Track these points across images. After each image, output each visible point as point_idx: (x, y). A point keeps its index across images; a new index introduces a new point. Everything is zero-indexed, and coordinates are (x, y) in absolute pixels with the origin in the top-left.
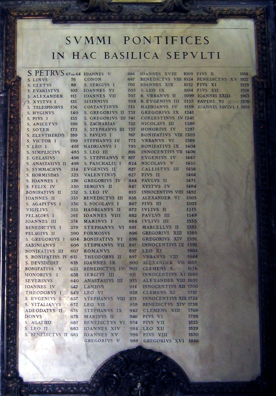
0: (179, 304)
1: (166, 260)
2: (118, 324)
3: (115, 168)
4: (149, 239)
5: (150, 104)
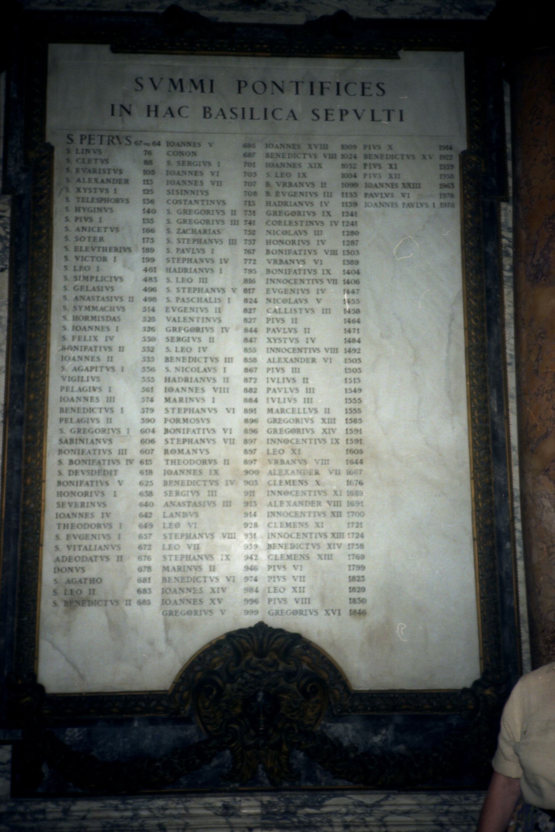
0: (332, 546)
1: (308, 466)
2: (223, 582)
4: (278, 431)
5: (281, 198)
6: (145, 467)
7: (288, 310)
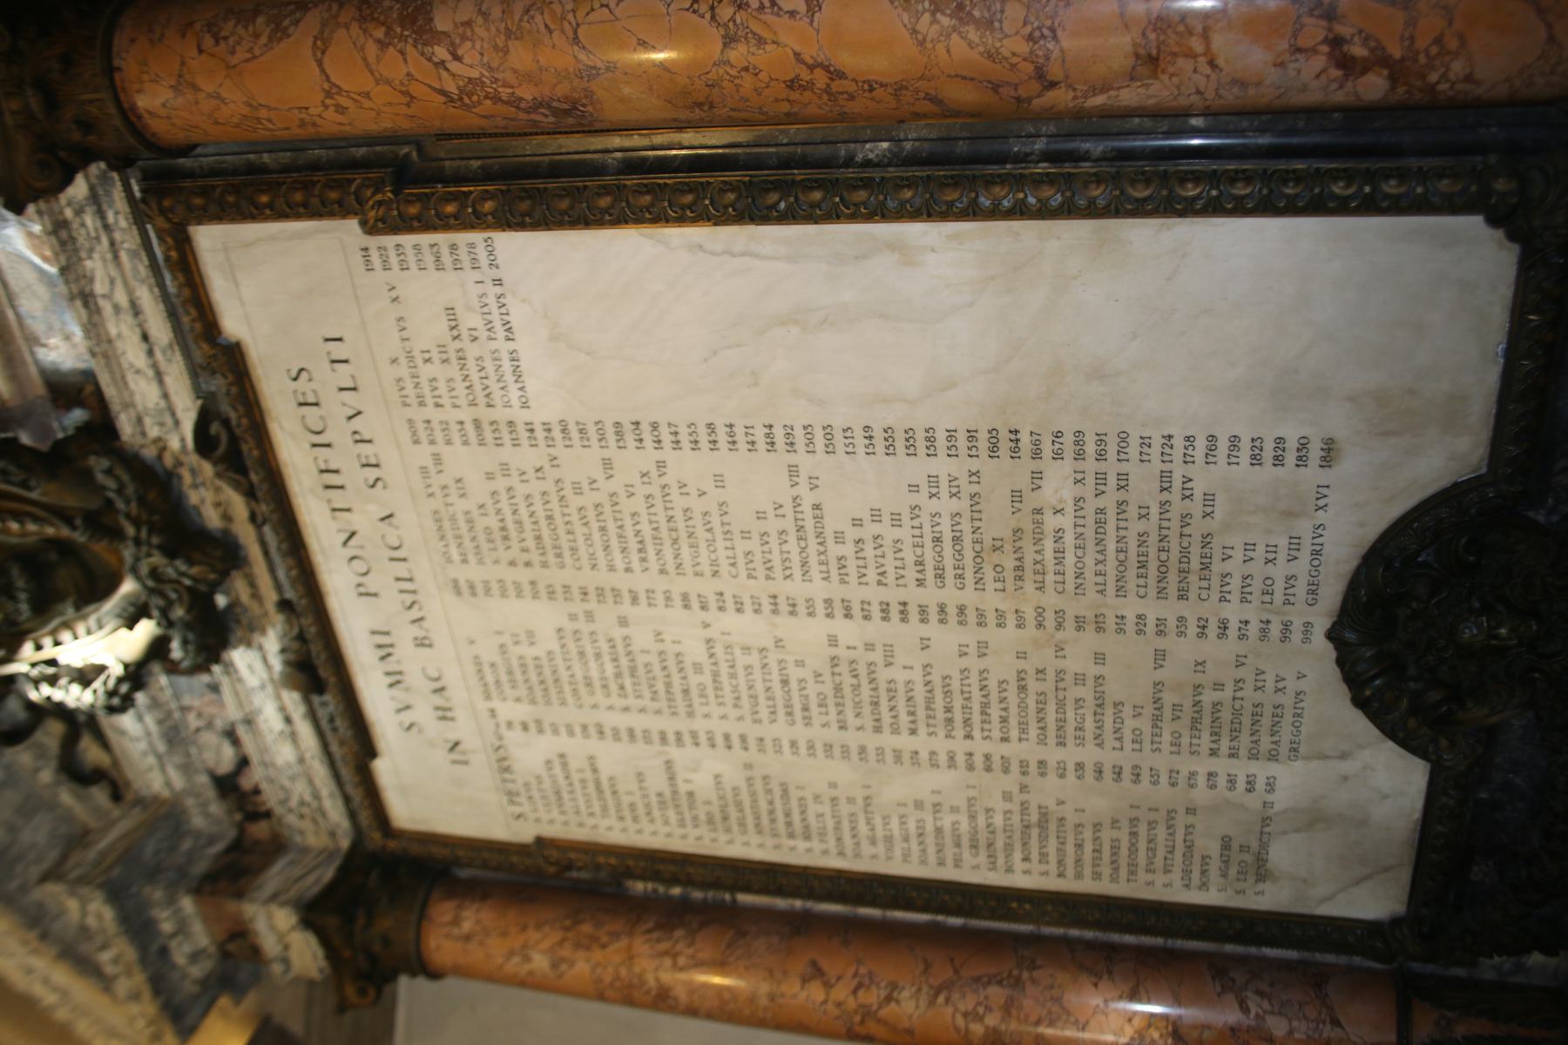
0: (1188, 493)
1: (1028, 526)
5: (531, 543)
7: (728, 544)
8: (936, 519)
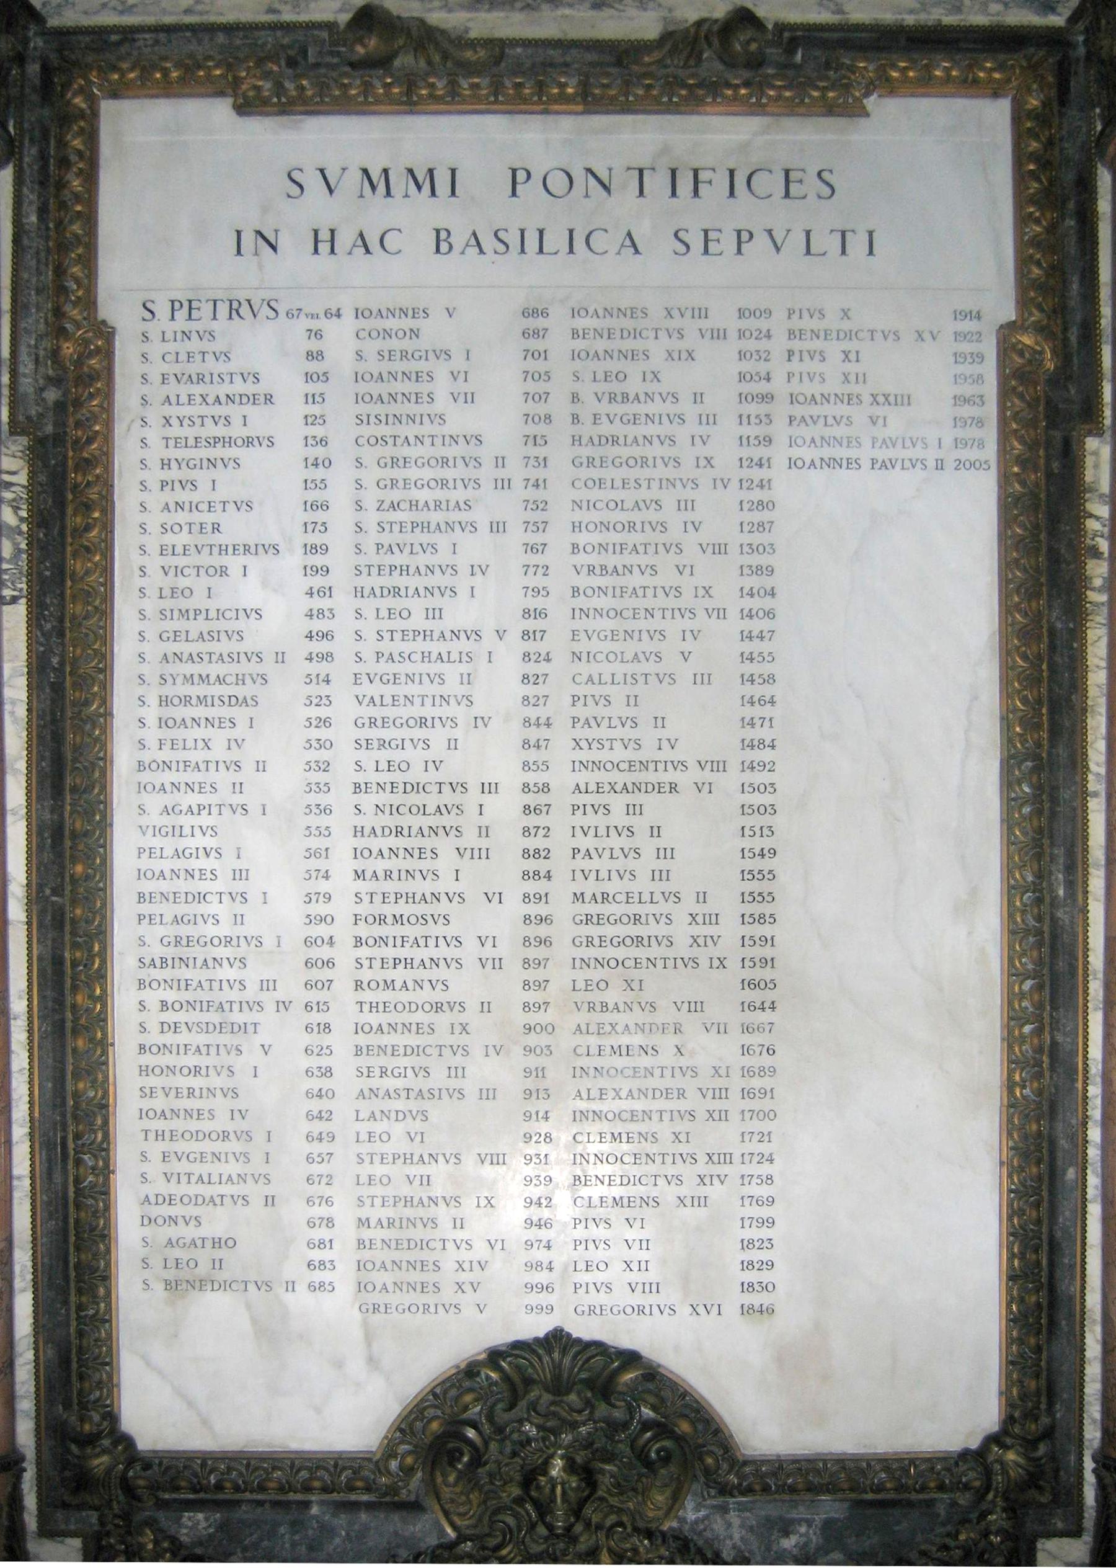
0: (707, 1180)
1: (659, 1018)
2: (481, 1251)
3: (469, 675)
4: (596, 942)
5: (605, 429)
6: (315, 1017)
7: (619, 678)
8: (664, 919)
